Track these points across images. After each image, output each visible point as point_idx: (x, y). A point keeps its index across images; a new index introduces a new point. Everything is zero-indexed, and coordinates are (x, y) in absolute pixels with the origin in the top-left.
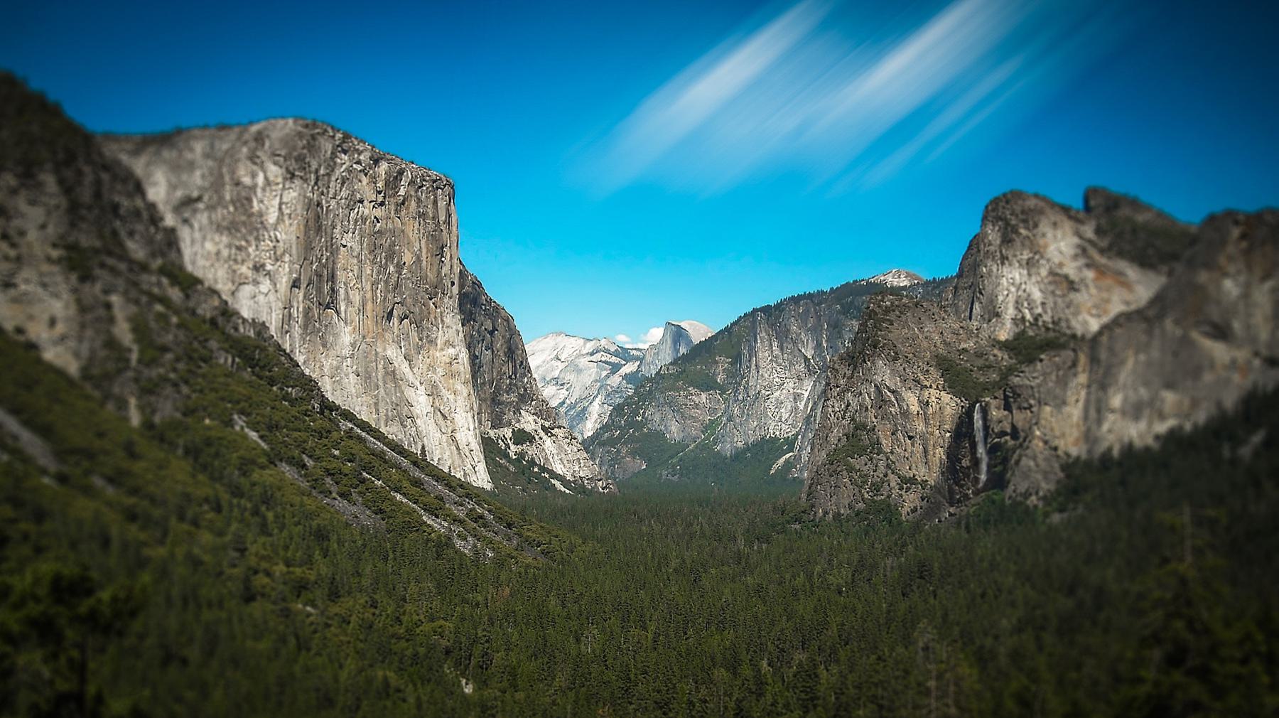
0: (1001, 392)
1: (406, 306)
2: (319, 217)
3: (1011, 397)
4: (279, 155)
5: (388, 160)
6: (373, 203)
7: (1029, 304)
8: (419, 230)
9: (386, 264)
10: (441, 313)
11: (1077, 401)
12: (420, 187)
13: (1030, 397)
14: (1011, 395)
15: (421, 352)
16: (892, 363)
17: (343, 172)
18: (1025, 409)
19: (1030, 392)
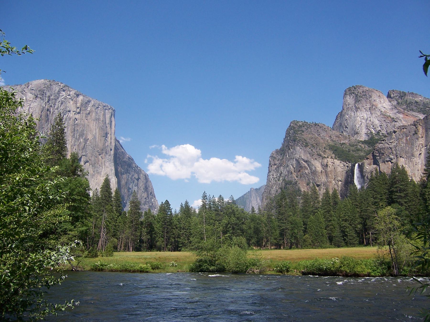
0: (371, 155)
1: (88, 157)
2: (48, 115)
3: (377, 156)
4: (33, 90)
5: (83, 96)
6: (75, 112)
7: (373, 126)
8: (96, 125)
9: (79, 138)
10: (104, 161)
11: (420, 154)
12: (97, 108)
13: (390, 154)
14: (378, 155)
15: (94, 177)
16: (304, 148)
17: (62, 99)
18: (387, 161)
19: (390, 151)
